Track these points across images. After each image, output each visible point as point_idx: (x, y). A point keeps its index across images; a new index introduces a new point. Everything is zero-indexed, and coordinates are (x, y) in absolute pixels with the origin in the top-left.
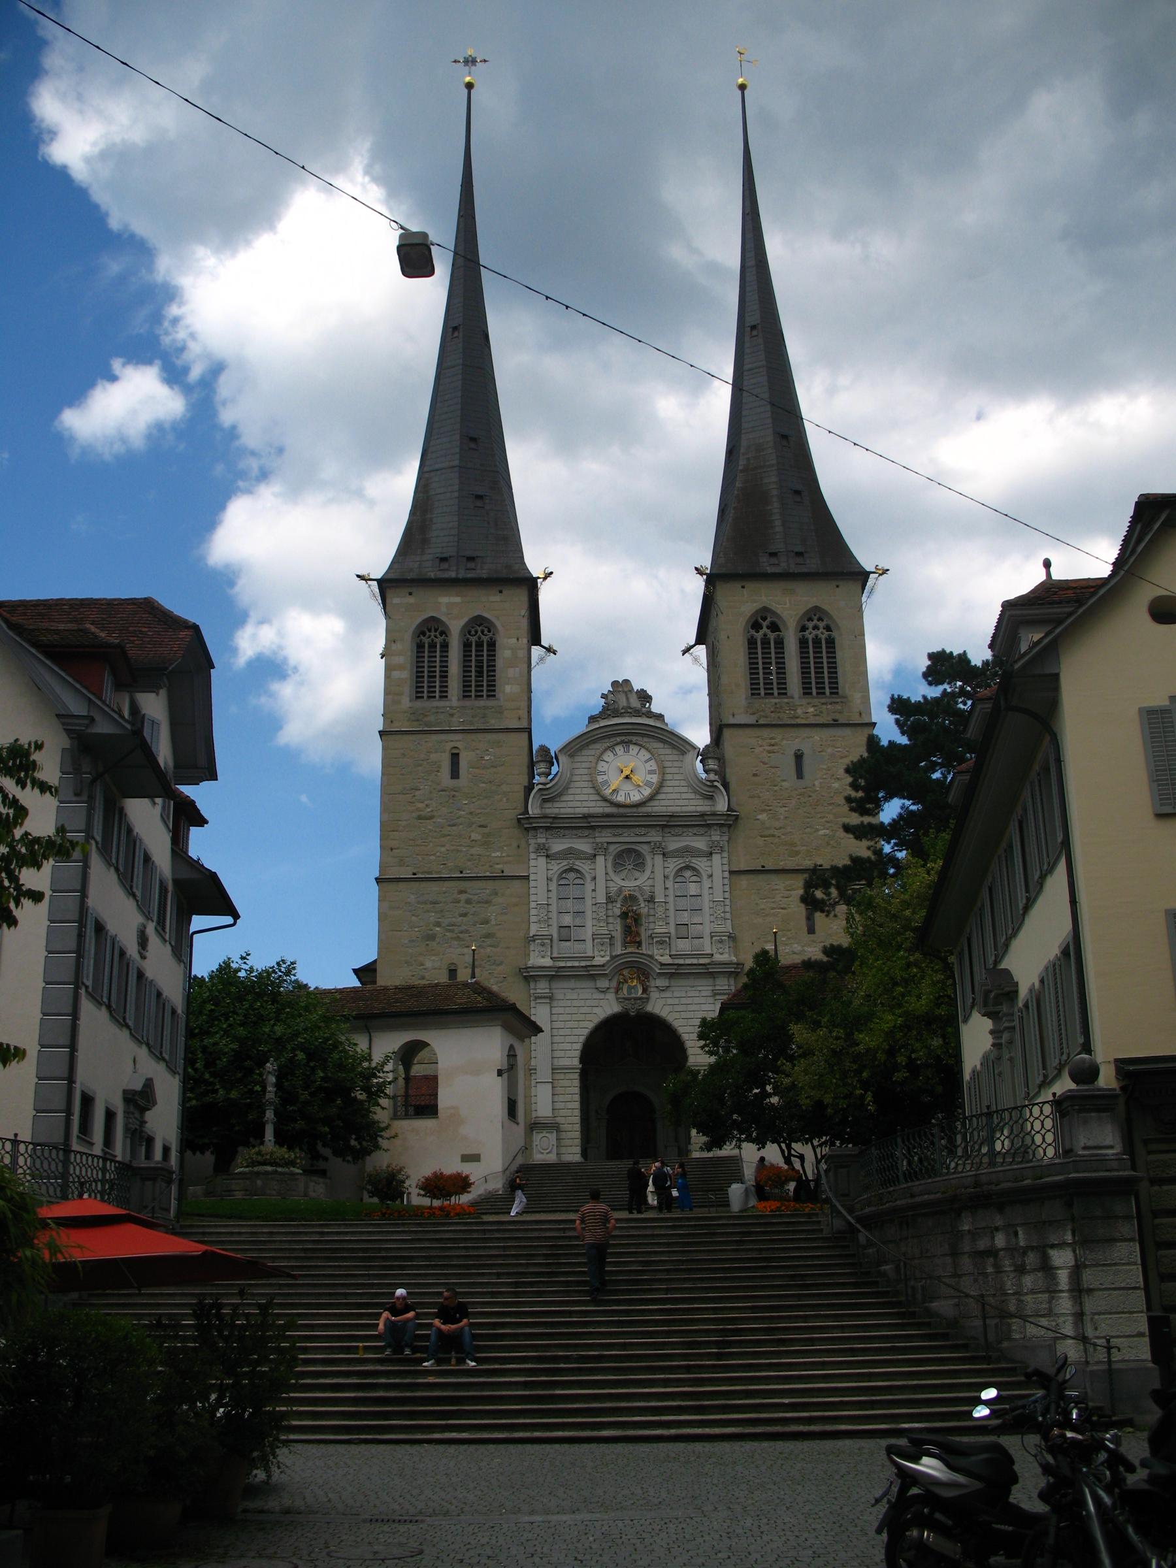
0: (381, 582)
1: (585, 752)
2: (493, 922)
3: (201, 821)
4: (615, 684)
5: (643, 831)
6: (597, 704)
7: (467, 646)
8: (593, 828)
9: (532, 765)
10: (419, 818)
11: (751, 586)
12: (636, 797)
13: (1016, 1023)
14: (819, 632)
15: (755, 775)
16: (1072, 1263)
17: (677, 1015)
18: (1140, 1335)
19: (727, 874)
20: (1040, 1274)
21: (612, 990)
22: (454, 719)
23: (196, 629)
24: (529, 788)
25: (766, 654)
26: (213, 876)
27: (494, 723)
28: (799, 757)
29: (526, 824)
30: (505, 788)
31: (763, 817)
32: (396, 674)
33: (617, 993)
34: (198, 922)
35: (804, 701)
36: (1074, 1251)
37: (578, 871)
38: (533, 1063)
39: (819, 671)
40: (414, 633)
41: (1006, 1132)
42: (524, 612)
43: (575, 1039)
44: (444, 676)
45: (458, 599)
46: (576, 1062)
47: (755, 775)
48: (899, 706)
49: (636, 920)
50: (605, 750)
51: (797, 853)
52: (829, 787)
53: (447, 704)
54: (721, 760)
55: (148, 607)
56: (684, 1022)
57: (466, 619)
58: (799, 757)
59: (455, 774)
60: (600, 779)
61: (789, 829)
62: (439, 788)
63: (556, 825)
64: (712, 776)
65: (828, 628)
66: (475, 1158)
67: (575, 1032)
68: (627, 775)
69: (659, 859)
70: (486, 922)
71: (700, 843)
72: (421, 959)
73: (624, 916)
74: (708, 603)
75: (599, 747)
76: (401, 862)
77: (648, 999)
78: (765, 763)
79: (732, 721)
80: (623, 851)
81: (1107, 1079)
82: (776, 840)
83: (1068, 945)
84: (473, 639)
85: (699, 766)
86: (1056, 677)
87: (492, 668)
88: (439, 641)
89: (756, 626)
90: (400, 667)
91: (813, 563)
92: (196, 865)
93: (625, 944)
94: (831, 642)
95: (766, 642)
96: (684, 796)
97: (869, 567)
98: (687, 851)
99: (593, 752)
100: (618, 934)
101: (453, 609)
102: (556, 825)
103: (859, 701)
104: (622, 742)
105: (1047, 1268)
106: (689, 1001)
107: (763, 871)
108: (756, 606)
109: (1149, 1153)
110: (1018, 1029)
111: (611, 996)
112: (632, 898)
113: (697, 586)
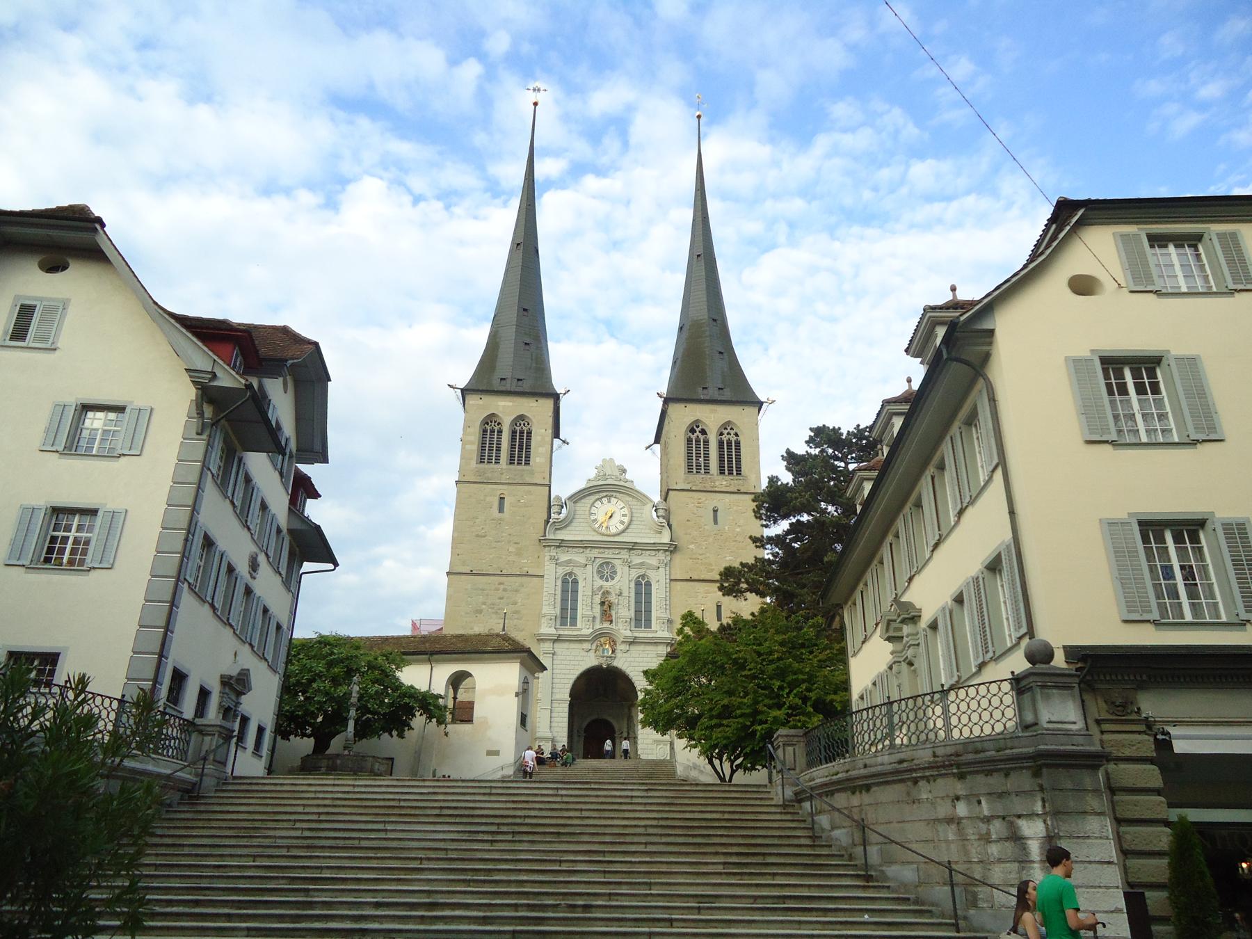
0: (462, 390)
3: (316, 495)
4: (604, 460)
6: (592, 473)
7: (514, 432)
9: (550, 507)
10: (478, 536)
11: (691, 407)
12: (613, 530)
13: (922, 641)
16: (1043, 833)
18: (1118, 911)
20: (1007, 844)
23: (316, 344)
24: (547, 521)
25: (698, 448)
26: (318, 528)
27: (528, 480)
28: (715, 511)
29: (544, 543)
31: (692, 546)
32: (468, 447)
34: (307, 566)
35: (721, 477)
36: (1045, 822)
39: (730, 460)
41: (904, 731)
42: (551, 413)
44: (498, 450)
48: (792, 459)
54: (667, 511)
55: (285, 330)
58: (715, 511)
59: (501, 510)
63: (561, 544)
64: (662, 520)
66: (497, 753)
68: (610, 516)
70: (515, 603)
71: (653, 561)
73: (603, 603)
74: (663, 414)
76: (464, 563)
81: (1059, 661)
83: (999, 555)
84: (518, 429)
85: (654, 514)
86: (992, 332)
87: (528, 447)
88: (496, 429)
89: (693, 431)
90: (471, 443)
91: (727, 394)
92: (307, 521)
93: (601, 622)
94: (738, 443)
95: (698, 441)
97: (762, 398)
100: (598, 615)
101: (507, 408)
102: (561, 544)
105: (1016, 838)
107: (691, 580)
108: (693, 419)
109: (1102, 732)
110: (922, 645)
111: (592, 654)
113: (660, 402)
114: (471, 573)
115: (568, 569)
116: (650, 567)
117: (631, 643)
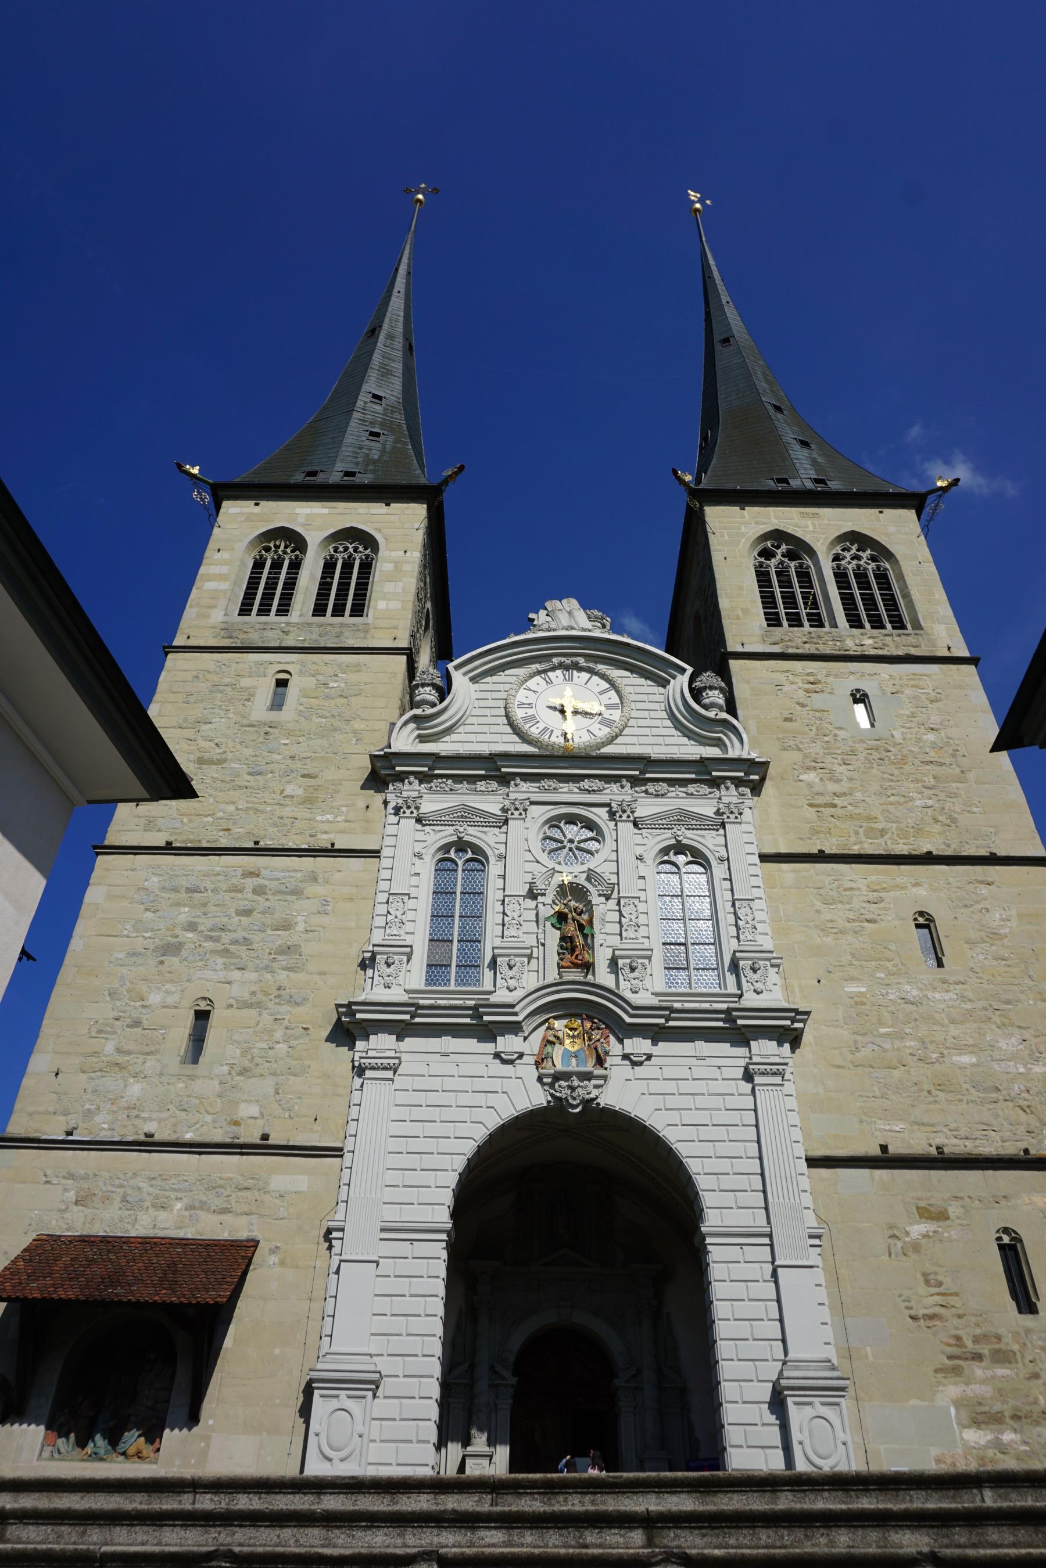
1: (495, 678)
2: (301, 927)
5: (597, 784)
7: (329, 567)
8: (505, 780)
14: (861, 563)
15: (786, 720)
17: (674, 1117)
19: (756, 860)
21: (532, 1060)
22: (291, 636)
30: (357, 725)
31: (810, 777)
33: (537, 1064)
37: (476, 849)
38: (340, 1216)
40: (253, 543)
43: (445, 1162)
45: (326, 511)
46: (442, 1217)
47: (786, 720)
49: (581, 927)
50: (531, 676)
51: (883, 832)
52: (919, 740)
53: (283, 619)
56: (690, 1133)
57: (332, 531)
59: (277, 704)
60: (519, 714)
61: (859, 795)
62: (245, 722)
63: (433, 768)
65: (873, 559)
67: (445, 1145)
69: (626, 828)
70: (287, 926)
72: (143, 987)
73: (561, 918)
75: (522, 672)
77: (605, 1078)
78: (802, 705)
79: (739, 649)
80: (559, 818)
82: (839, 812)
90: (222, 577)
94: (882, 578)
96: (669, 740)
98: (684, 818)
99: (513, 679)
103: (944, 634)
104: (561, 666)
106: (700, 1087)
107: (821, 857)
111: (527, 1071)
112: (576, 891)
114: (168, 849)
115: (448, 835)
116: (699, 822)
117: (658, 1034)
